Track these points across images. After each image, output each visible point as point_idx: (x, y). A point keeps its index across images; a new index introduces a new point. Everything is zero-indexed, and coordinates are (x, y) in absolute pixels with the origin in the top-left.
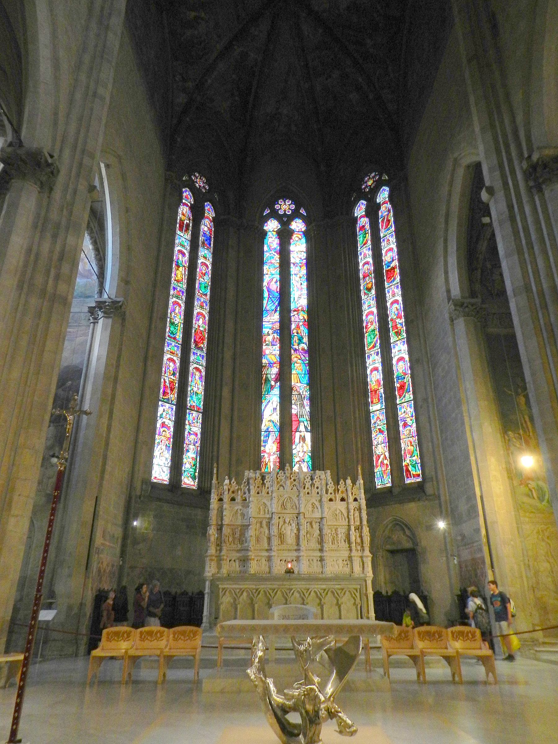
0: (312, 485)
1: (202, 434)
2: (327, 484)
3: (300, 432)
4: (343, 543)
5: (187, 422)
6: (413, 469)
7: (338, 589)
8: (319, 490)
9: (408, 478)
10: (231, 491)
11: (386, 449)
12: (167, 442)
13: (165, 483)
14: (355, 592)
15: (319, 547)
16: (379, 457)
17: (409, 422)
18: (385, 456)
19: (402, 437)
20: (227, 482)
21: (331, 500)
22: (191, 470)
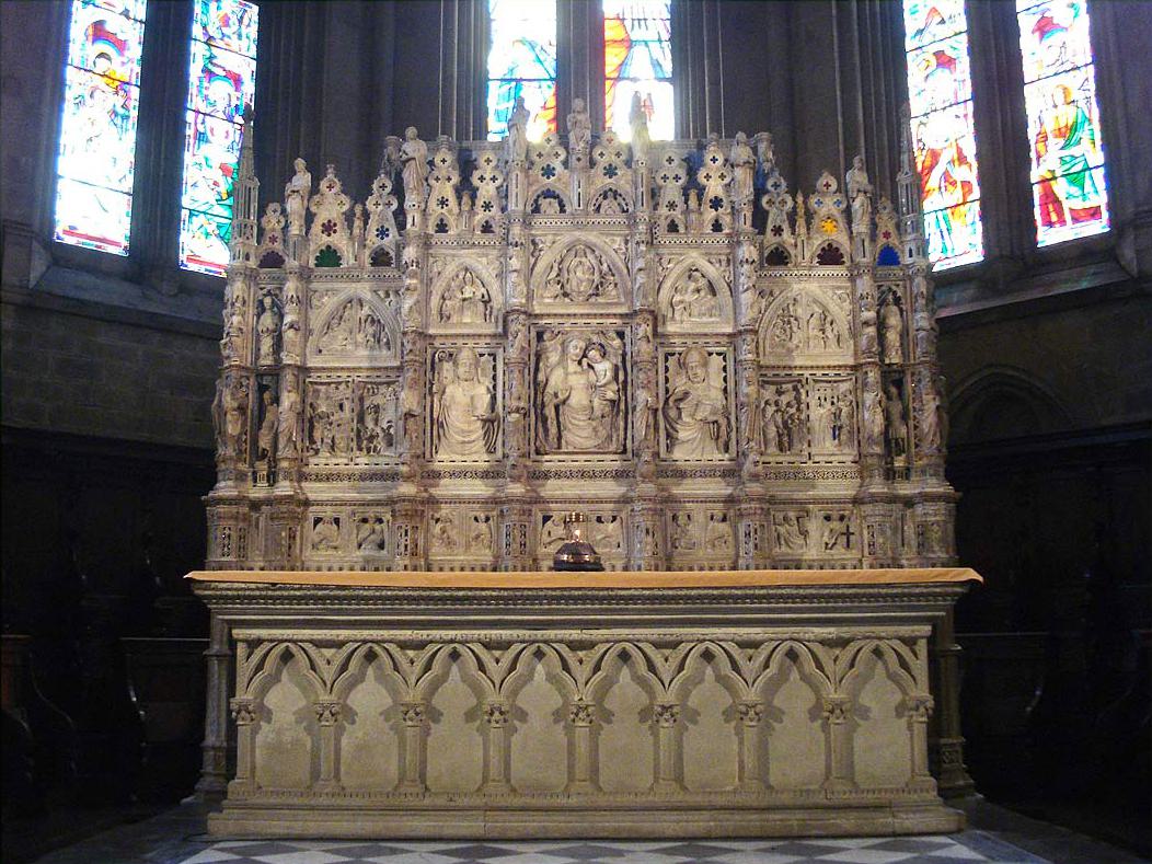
0: (693, 187)
1: (261, 78)
2: (759, 191)
3: (634, 80)
4: (830, 444)
5: (196, 30)
6: (1075, 190)
7: (823, 642)
8: (724, 214)
9: (1050, 224)
10: (317, 228)
11: (968, 127)
12: (119, 100)
13: (111, 250)
14: (904, 650)
15: (719, 458)
16: (935, 156)
17: (1059, 13)
18: (959, 151)
19: (1030, 70)
20: (302, 180)
21: (778, 258)
22: (218, 210)
